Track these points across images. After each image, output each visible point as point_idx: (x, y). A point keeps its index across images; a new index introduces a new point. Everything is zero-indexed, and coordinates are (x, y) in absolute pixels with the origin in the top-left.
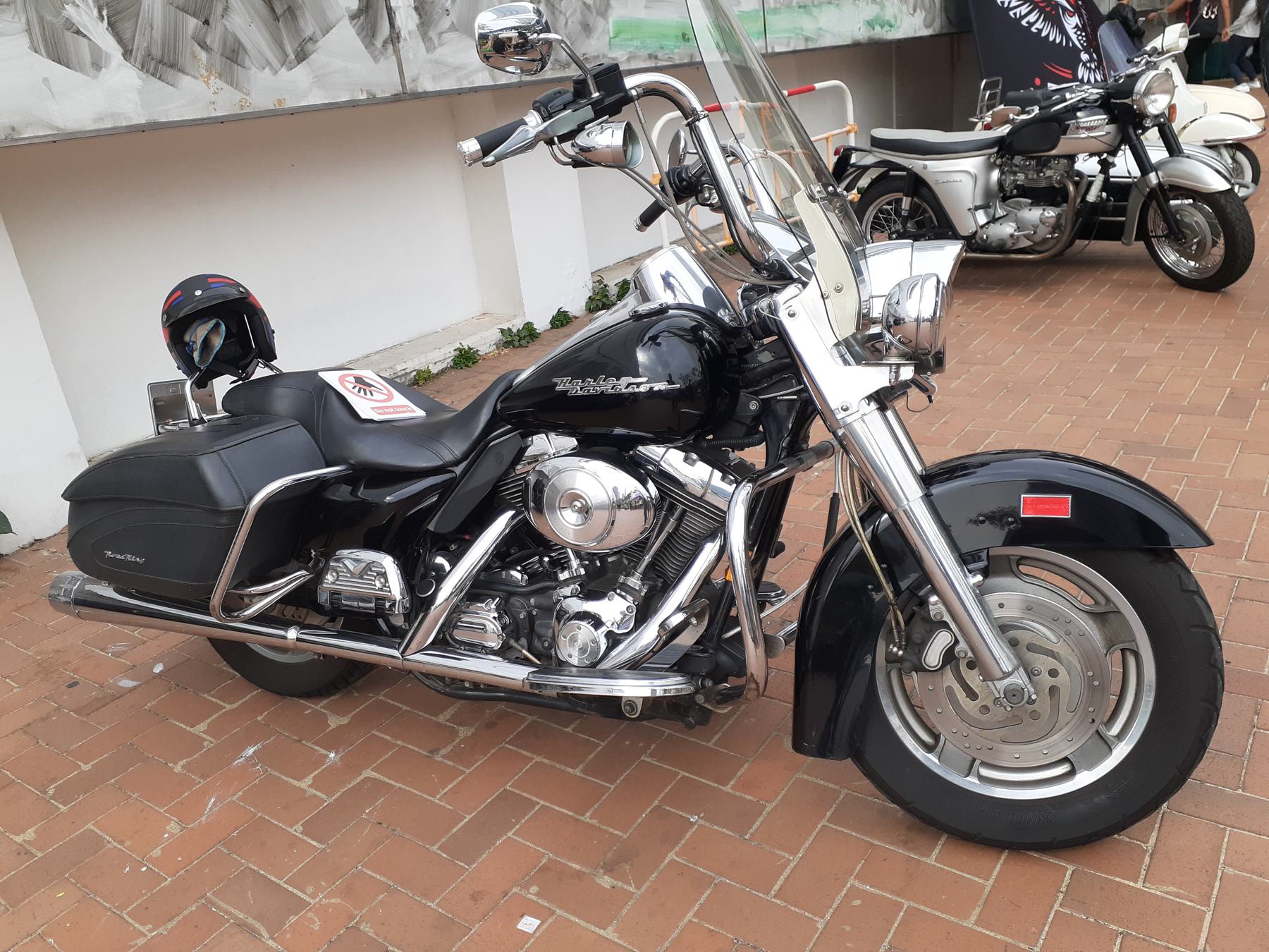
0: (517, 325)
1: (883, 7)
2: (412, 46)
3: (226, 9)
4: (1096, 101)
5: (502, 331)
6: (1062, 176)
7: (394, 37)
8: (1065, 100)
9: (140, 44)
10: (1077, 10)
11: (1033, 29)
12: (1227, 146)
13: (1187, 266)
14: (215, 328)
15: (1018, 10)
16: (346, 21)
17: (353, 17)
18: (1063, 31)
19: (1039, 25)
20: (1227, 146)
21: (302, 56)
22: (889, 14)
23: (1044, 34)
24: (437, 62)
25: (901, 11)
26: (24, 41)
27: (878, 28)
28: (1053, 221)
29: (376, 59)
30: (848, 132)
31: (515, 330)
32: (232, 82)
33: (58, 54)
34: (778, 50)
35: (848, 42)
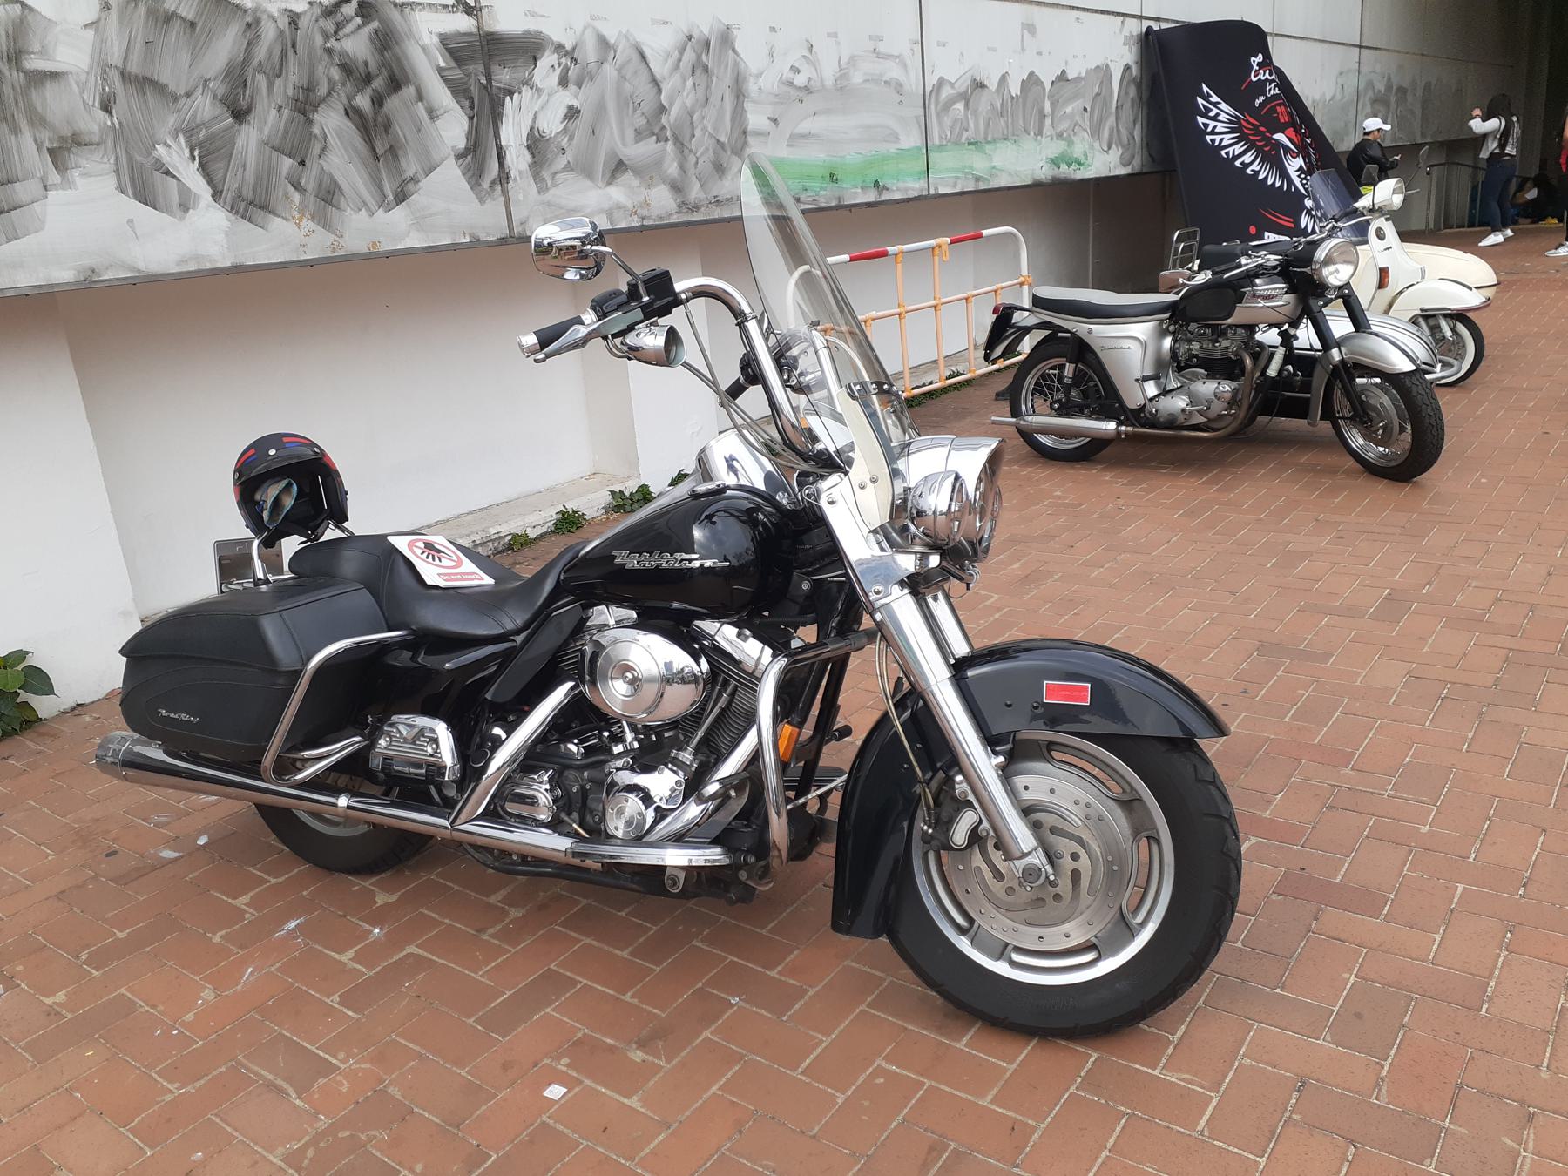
0: (630, 487)
1: (1070, 143)
2: (523, 188)
3: (324, 149)
4: (1275, 268)
5: (613, 493)
6: (1239, 347)
7: (504, 177)
8: (1240, 266)
9: (230, 186)
10: (1302, 150)
11: (1249, 171)
12: (1445, 316)
13: (1374, 452)
14: (292, 487)
16: (452, 160)
17: (460, 156)
18: (1284, 174)
19: (1255, 167)
20: (1445, 316)
21: (401, 197)
22: (1078, 150)
23: (1261, 176)
24: (549, 204)
25: (1092, 147)
26: (111, 181)
27: (1064, 167)
28: (1228, 396)
29: (482, 201)
30: (1021, 284)
31: (627, 493)
32: (325, 224)
33: (145, 195)
34: (942, 191)
35: (1028, 182)
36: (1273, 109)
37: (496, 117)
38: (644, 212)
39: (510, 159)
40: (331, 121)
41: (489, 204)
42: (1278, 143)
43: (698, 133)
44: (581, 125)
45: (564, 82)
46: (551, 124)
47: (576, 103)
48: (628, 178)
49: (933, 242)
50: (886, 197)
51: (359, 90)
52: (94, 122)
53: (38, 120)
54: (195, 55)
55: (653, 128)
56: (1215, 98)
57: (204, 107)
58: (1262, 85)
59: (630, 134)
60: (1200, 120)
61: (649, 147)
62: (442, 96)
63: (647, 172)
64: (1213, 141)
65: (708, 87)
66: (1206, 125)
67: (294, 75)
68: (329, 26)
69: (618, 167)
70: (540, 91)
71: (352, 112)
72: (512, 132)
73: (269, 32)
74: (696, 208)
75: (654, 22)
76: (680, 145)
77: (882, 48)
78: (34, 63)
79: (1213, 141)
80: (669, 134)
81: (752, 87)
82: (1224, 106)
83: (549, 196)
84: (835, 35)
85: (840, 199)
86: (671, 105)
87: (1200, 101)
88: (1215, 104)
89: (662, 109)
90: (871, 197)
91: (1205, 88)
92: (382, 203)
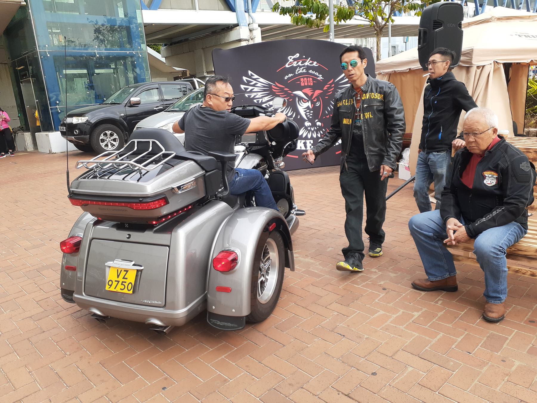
15: (260, 100)
36: (299, 80)
42: (296, 96)
56: (256, 76)
58: (292, 69)
60: (242, 87)
64: (249, 96)
66: (246, 89)
79: (249, 96)
82: (261, 80)
87: (245, 78)
88: (255, 79)
91: (250, 72)
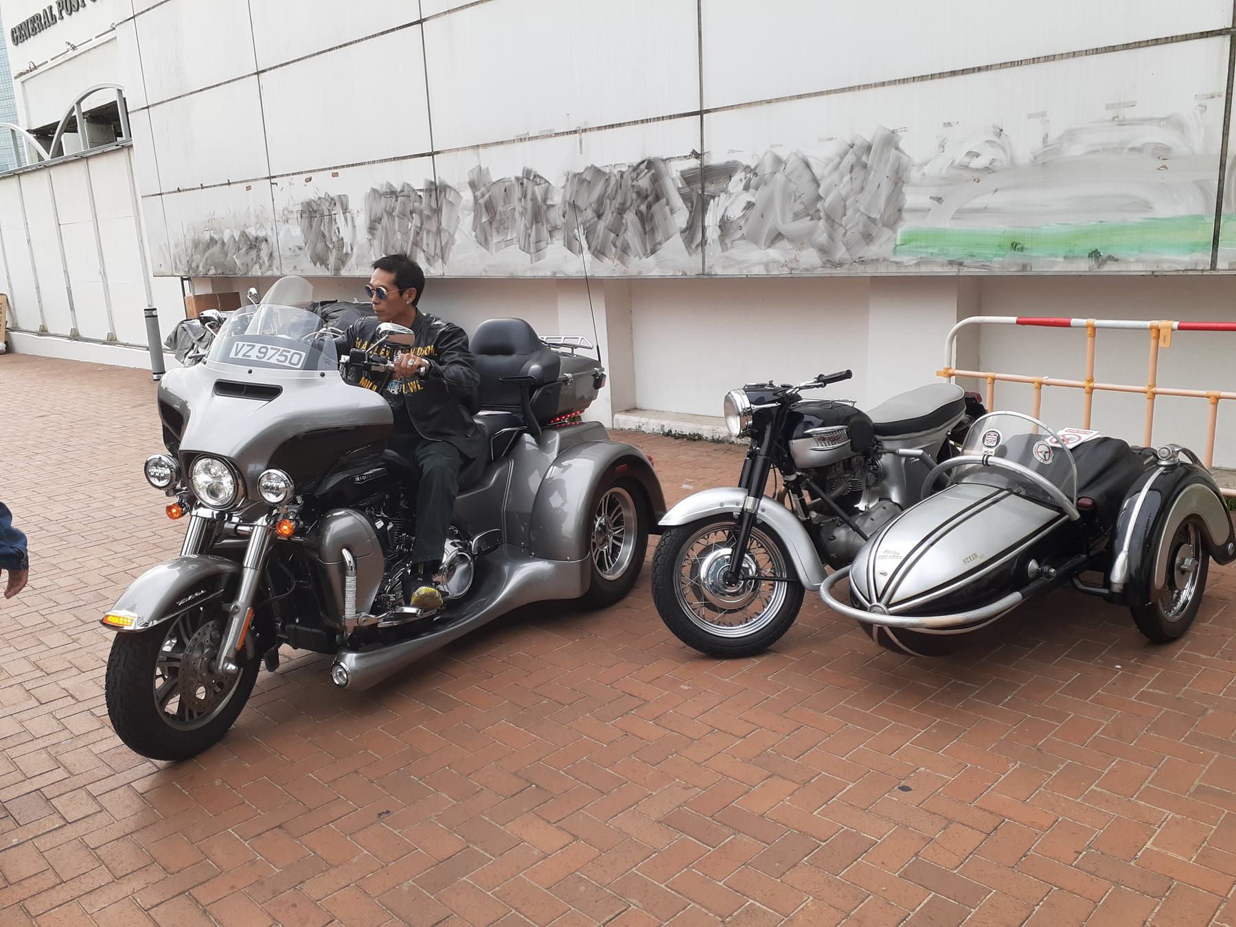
2: (713, 248)
7: (703, 243)
9: (594, 244)
16: (678, 234)
17: (682, 232)
21: (653, 252)
29: (690, 254)
37: (704, 210)
38: (794, 266)
39: (708, 233)
40: (630, 217)
41: (694, 256)
43: (849, 213)
44: (754, 213)
45: (746, 188)
46: (735, 213)
47: (753, 200)
48: (784, 244)
49: (1148, 324)
50: (1110, 268)
51: (642, 202)
52: (560, 221)
53: (548, 221)
54: (590, 192)
55: (810, 210)
57: (589, 214)
59: (789, 216)
61: (805, 223)
62: (677, 201)
63: (798, 241)
65: (865, 179)
67: (619, 199)
68: (634, 175)
69: (777, 237)
70: (731, 194)
71: (639, 213)
72: (712, 219)
73: (613, 181)
74: (841, 264)
75: (820, 140)
76: (831, 221)
77: (1129, 114)
78: (549, 202)
80: (822, 214)
81: (914, 175)
83: (727, 253)
84: (1043, 115)
85: (1024, 267)
86: (827, 195)
89: (819, 198)
90: (1083, 266)
92: (646, 255)
